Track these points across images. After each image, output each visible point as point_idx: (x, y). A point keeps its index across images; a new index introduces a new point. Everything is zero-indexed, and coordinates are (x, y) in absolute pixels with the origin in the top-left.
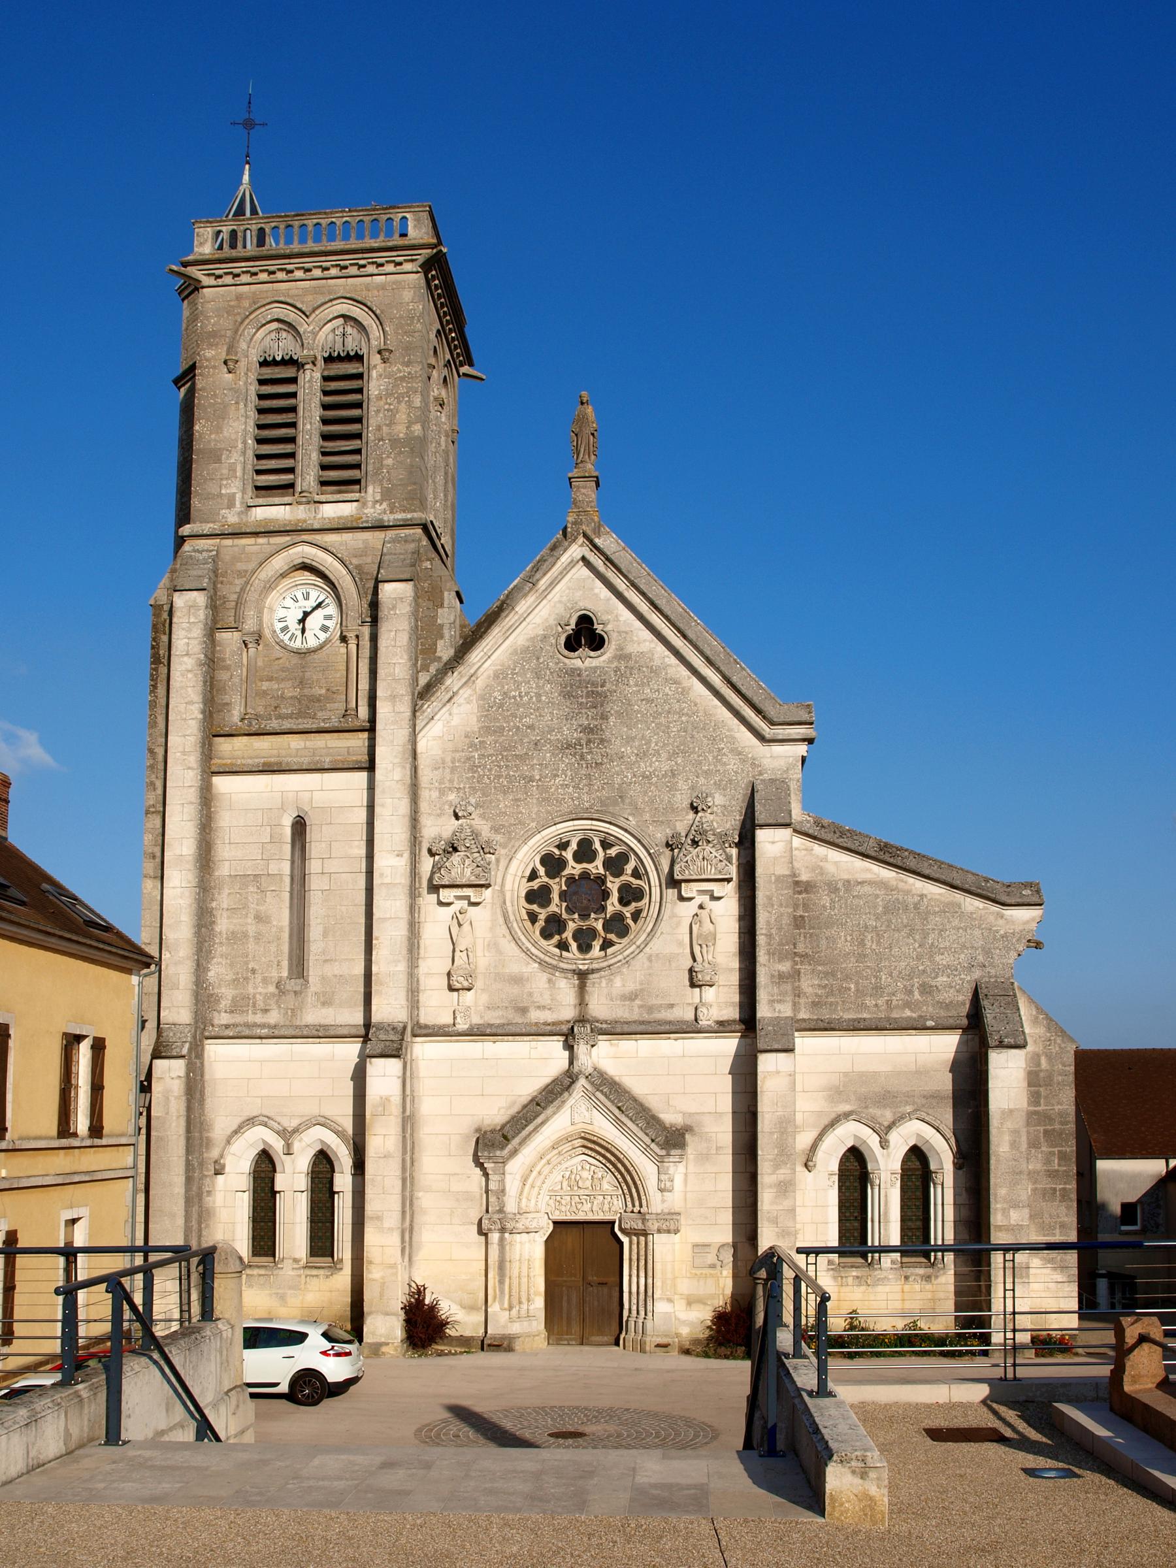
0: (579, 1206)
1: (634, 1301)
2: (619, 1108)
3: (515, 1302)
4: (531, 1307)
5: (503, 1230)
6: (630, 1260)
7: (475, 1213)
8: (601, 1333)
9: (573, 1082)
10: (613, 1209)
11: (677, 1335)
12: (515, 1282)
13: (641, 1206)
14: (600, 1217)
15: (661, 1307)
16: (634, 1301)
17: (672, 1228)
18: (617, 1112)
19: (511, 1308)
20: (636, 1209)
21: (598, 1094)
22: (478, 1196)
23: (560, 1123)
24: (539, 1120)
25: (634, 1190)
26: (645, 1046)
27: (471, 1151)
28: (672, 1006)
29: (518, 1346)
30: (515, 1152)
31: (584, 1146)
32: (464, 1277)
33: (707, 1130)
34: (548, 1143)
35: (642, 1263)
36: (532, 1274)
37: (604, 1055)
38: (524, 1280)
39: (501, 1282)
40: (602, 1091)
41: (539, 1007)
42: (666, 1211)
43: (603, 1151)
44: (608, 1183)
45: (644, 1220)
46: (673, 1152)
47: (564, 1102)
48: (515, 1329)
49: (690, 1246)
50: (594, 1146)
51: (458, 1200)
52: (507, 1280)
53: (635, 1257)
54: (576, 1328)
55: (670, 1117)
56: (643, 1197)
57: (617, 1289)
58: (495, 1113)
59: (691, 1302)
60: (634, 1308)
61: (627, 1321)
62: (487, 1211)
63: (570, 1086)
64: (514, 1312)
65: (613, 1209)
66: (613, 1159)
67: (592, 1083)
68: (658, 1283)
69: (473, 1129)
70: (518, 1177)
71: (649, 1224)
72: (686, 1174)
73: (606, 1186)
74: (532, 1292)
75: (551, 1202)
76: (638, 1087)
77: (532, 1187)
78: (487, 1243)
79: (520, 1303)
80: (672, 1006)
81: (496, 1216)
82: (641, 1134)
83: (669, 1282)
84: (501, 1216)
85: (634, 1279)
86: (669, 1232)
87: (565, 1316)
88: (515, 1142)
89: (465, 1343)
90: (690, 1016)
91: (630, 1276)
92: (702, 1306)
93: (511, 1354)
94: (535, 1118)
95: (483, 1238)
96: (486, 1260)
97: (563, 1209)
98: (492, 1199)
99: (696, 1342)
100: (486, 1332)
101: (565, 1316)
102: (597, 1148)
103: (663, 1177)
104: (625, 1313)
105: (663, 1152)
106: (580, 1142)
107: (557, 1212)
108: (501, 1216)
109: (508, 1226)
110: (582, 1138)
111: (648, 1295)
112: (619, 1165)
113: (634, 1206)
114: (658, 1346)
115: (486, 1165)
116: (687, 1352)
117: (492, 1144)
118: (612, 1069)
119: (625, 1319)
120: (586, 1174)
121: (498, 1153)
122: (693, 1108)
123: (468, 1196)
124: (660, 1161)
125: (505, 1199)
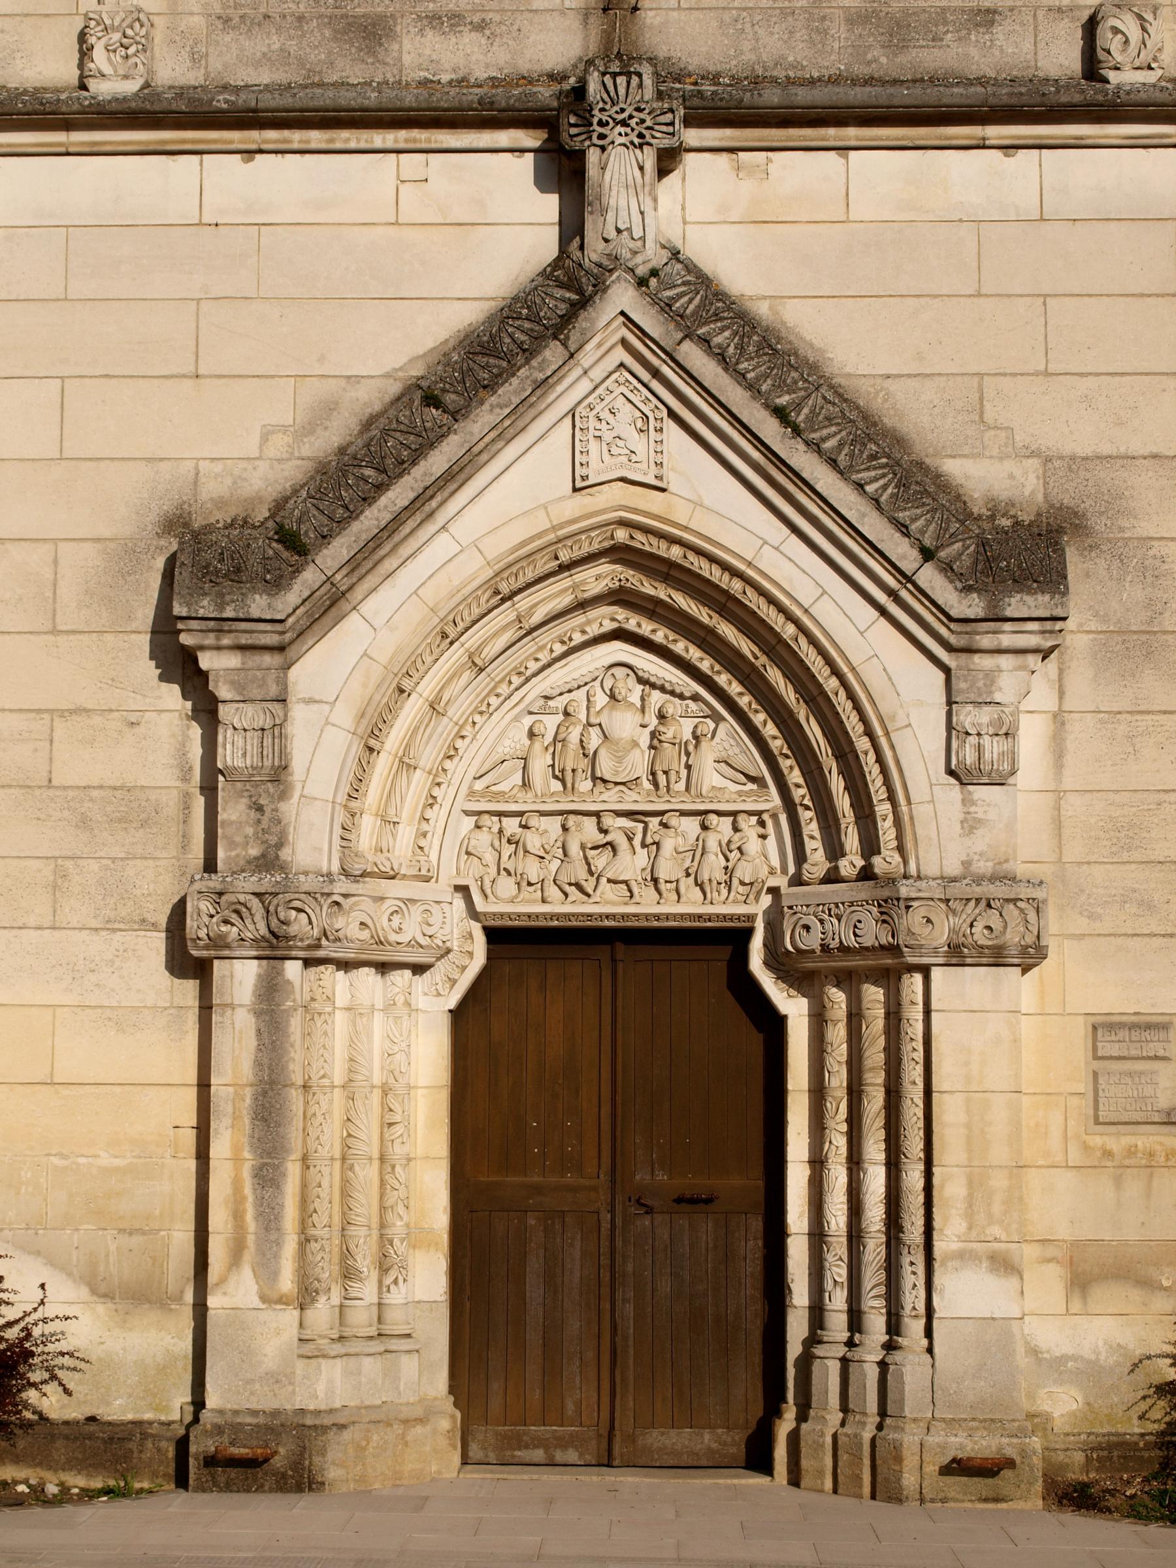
0: (600, 860)
1: (837, 1270)
2: (780, 413)
3: (326, 1269)
4: (396, 1297)
5: (274, 947)
6: (818, 1092)
7: (157, 880)
8: (690, 1418)
9: (583, 303)
10: (744, 872)
11: (1038, 1422)
12: (328, 1177)
13: (870, 846)
14: (687, 905)
15: (965, 1294)
16: (837, 1270)
17: (1013, 937)
18: (770, 429)
19: (306, 1296)
20: (851, 863)
21: (693, 355)
22: (170, 802)
23: (522, 488)
24: (437, 462)
25: (837, 784)
26: (880, 177)
27: (146, 614)
28: (987, 18)
29: (335, 1466)
30: (330, 605)
31: (620, 597)
32: (106, 1160)
33: (1146, 528)
34: (473, 570)
35: (874, 1102)
36: (398, 1151)
37: (711, 210)
38: (367, 1174)
39: (267, 1177)
40: (705, 342)
41: (434, 20)
42: (983, 867)
43: (703, 614)
44: (721, 761)
45: (889, 907)
46: (1016, 605)
47: (542, 385)
48: (326, 1387)
49: (1079, 1031)
50: (667, 593)
51: (84, 823)
52: (293, 1169)
53: (837, 1080)
54: (580, 1393)
55: (990, 477)
56: (883, 809)
57: (757, 1224)
58: (248, 452)
59: (1088, 1273)
60: (837, 1301)
61: (806, 1361)
62: (210, 866)
63: (568, 319)
64: (322, 1313)
65: (744, 872)
66: (745, 646)
67: (666, 307)
68: (951, 1187)
69: (152, 517)
70: (344, 715)
71: (914, 919)
72: (1059, 719)
73: (711, 777)
74: (397, 1228)
75: (483, 841)
76: (852, 344)
77: (405, 765)
78: (206, 1008)
79: (348, 1274)
80: (987, 18)
81: (249, 883)
82: (874, 526)
83: (999, 1181)
84: (267, 882)
85: (837, 1176)
86: (996, 957)
87: (533, 1338)
88: (334, 554)
89: (110, 1453)
90: (1061, 57)
91: (818, 1163)
92: (1136, 1294)
93: (301, 1506)
94: (418, 455)
95: (191, 987)
96: (204, 1085)
97: (533, 870)
98: (232, 811)
99: (1112, 1452)
100: (199, 1403)
101: (533, 1338)
102: (682, 601)
103: (967, 717)
104: (797, 1328)
105: (973, 606)
106: (600, 577)
107: (506, 886)
108: (267, 882)
109: (299, 925)
110: (619, 553)
111: (906, 1237)
112: (775, 676)
113: (835, 851)
114: (958, 1467)
115: (206, 661)
116: (1075, 1498)
117: (230, 584)
118: (738, 266)
119: (794, 1349)
120: (627, 725)
121: (258, 605)
122: (1082, 435)
123: (127, 807)
124: (951, 647)
125: (289, 808)
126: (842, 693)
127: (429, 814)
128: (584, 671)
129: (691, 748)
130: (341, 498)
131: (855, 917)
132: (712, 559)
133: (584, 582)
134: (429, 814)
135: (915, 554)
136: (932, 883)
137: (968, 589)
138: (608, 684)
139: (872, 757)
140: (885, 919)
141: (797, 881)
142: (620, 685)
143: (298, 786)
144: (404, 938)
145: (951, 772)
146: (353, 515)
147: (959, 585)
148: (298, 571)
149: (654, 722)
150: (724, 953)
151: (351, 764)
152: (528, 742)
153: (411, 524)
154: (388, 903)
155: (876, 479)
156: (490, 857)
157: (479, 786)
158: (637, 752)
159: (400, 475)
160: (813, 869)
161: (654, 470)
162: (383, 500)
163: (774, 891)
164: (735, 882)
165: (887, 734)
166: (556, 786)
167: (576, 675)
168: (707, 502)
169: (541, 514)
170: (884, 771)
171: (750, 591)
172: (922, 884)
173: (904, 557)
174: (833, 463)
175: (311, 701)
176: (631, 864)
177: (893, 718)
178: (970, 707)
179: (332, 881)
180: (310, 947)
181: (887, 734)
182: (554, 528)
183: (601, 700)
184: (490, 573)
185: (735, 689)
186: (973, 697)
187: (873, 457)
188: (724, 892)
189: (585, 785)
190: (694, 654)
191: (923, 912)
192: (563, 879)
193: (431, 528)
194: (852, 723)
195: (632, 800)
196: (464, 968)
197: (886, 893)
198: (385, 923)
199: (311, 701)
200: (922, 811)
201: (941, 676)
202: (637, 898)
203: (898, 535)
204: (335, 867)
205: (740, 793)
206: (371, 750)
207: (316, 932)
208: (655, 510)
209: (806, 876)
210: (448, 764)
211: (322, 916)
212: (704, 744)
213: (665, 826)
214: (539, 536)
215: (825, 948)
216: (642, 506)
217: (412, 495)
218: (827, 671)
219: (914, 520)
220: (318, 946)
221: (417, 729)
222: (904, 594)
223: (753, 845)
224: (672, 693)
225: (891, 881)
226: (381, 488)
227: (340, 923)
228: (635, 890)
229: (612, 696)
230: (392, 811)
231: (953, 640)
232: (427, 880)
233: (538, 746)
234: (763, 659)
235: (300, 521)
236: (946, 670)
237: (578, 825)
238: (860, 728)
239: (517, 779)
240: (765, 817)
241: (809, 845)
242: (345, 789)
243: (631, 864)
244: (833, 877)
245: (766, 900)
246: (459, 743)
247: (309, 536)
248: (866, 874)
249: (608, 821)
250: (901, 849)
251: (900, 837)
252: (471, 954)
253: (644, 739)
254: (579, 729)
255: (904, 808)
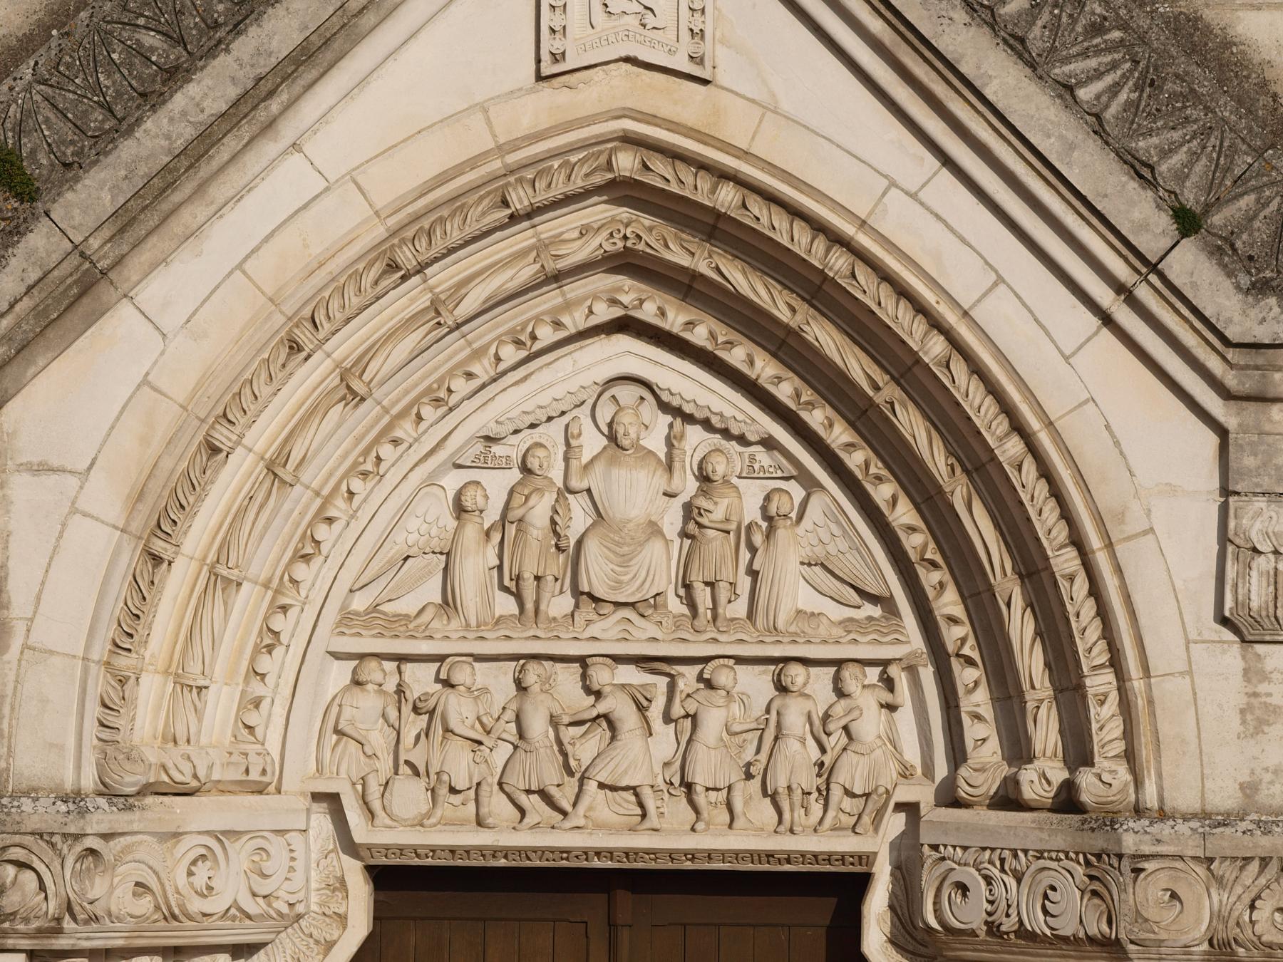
10: (853, 773)
13: (1079, 751)
14: (748, 834)
20: (1044, 776)
25: (1021, 627)
31: (628, 262)
34: (350, 225)
44: (814, 563)
45: (1104, 869)
56: (1099, 682)
66: (857, 366)
70: (106, 497)
73: (795, 592)
75: (366, 710)
77: (219, 578)
107: (410, 796)
112: (912, 424)
113: (1018, 749)
120: (637, 493)
126: (1030, 467)
127: (265, 664)
128: (559, 391)
129: (758, 539)
130: (98, 88)
131: (1046, 879)
132: (795, 212)
133: (558, 240)
134: (265, 664)
135: (1164, 222)
136: (1183, 828)
137: (1260, 288)
138: (605, 414)
139: (1081, 586)
140: (1096, 889)
141: (950, 798)
142: (626, 418)
143: (19, 629)
144: (215, 905)
145: (1224, 621)
146: (123, 127)
147: (1245, 280)
148: (17, 231)
149: (692, 485)
150: (823, 909)
151: (119, 587)
152: (452, 524)
153: (231, 144)
154: (187, 842)
155: (1098, 74)
156: (379, 739)
157: (360, 603)
158: (657, 546)
159: (211, 53)
160: (978, 779)
161: (687, 45)
162: (179, 101)
163: (910, 809)
164: (836, 792)
165: (1109, 545)
166: (506, 605)
167: (544, 399)
168: (785, 106)
169: (477, 120)
170: (1103, 612)
171: (863, 273)
172: (1164, 830)
173: (1143, 227)
174: (1016, 44)
175: (43, 469)
176: (644, 754)
177: (1121, 517)
178: (1260, 503)
179: (83, 812)
180: (40, 933)
181: (1109, 545)
182: (501, 150)
183: (591, 442)
184: (380, 232)
185: (839, 435)
186: (1267, 483)
187: (1096, 29)
188: (817, 809)
189: (560, 604)
190: (764, 369)
191: (1163, 880)
192: (516, 781)
193: (269, 148)
194: (1047, 522)
195: (646, 637)
196: (330, 945)
197: (1098, 842)
198: (181, 879)
199: (43, 469)
200: (1170, 691)
201: (1213, 440)
202: (653, 820)
203: (1133, 185)
204: (89, 781)
205: (847, 624)
206: (157, 560)
207: (52, 907)
208: (689, 116)
209: (963, 791)
210: (301, 571)
211: (64, 877)
212: (782, 533)
213: (709, 685)
214: (473, 163)
215: (993, 929)
216: (666, 111)
217: (233, 92)
218: (1002, 425)
219: (1165, 153)
220: (57, 931)
221: (242, 511)
222: (1143, 293)
223: (871, 723)
224: (726, 433)
225: (1109, 819)
226: (175, 75)
227: (98, 888)
228: (651, 804)
229: (612, 438)
230: (194, 667)
231: (1231, 380)
232: (260, 790)
233: (471, 532)
234: (890, 391)
235: (19, 130)
236: (1222, 432)
237: (546, 680)
238: (1061, 532)
239: (431, 591)
240: (894, 671)
241: (972, 731)
242: (108, 631)
243: (644, 754)
244: (1007, 799)
245: (895, 824)
246: (322, 532)
247: (40, 164)
248: (1067, 801)
249: (601, 675)
250: (1130, 756)
251: (1129, 734)
252: (342, 919)
253: (672, 521)
254: (549, 498)
255: (1137, 684)
